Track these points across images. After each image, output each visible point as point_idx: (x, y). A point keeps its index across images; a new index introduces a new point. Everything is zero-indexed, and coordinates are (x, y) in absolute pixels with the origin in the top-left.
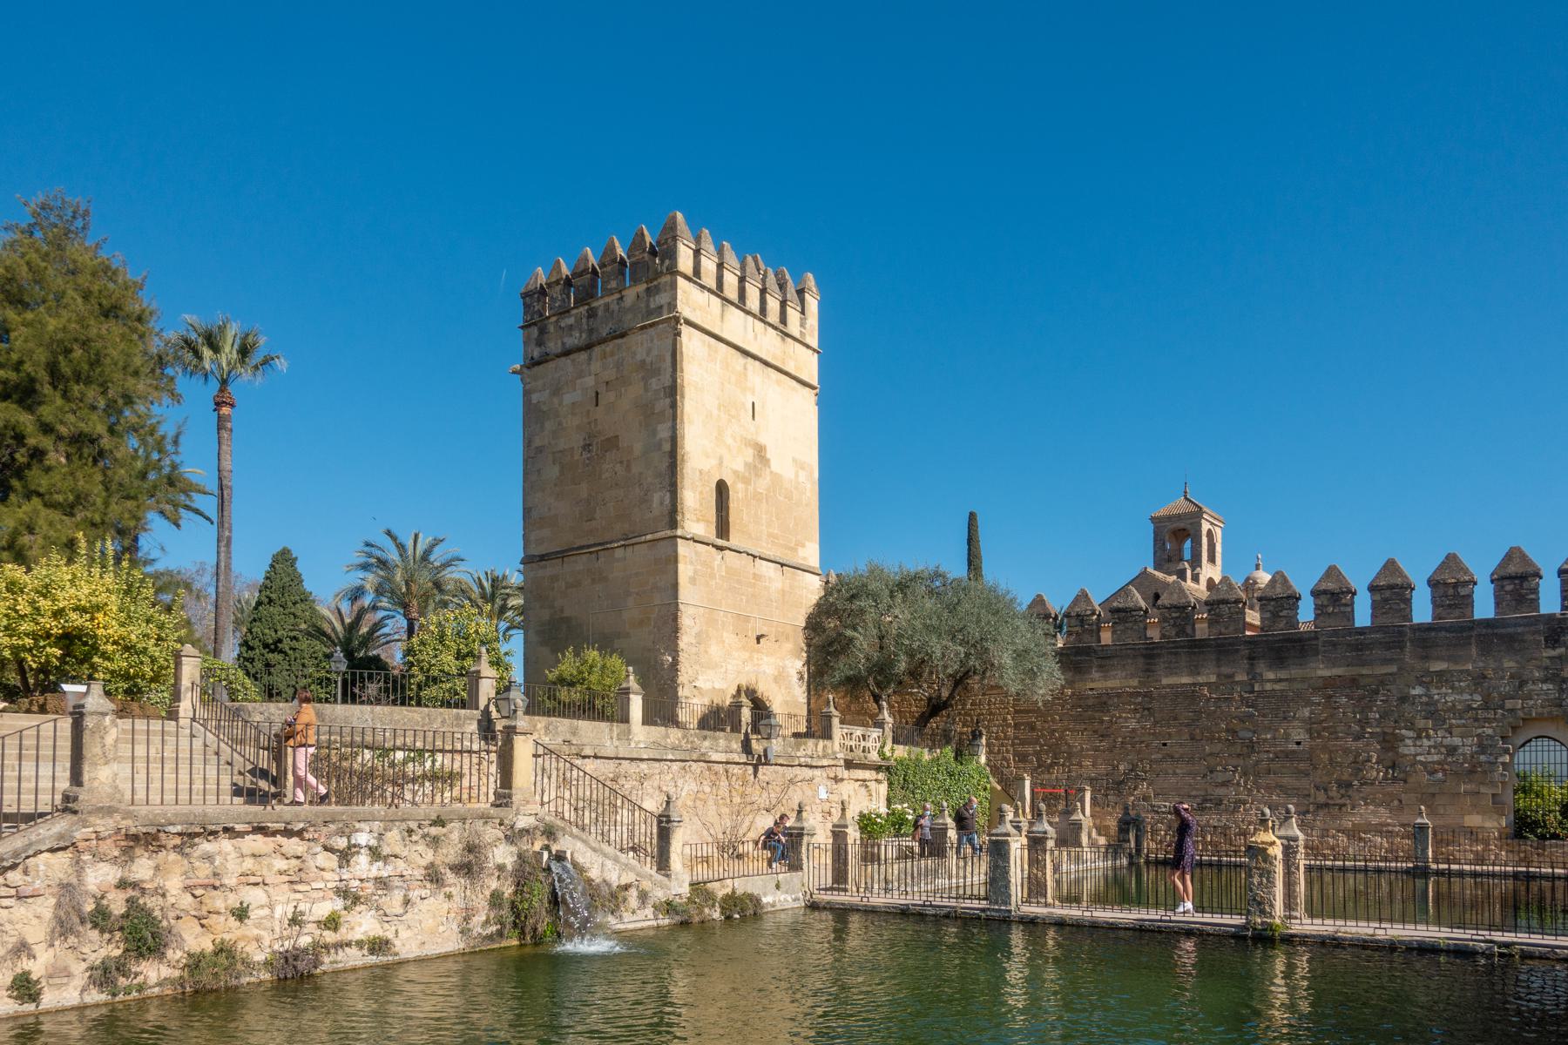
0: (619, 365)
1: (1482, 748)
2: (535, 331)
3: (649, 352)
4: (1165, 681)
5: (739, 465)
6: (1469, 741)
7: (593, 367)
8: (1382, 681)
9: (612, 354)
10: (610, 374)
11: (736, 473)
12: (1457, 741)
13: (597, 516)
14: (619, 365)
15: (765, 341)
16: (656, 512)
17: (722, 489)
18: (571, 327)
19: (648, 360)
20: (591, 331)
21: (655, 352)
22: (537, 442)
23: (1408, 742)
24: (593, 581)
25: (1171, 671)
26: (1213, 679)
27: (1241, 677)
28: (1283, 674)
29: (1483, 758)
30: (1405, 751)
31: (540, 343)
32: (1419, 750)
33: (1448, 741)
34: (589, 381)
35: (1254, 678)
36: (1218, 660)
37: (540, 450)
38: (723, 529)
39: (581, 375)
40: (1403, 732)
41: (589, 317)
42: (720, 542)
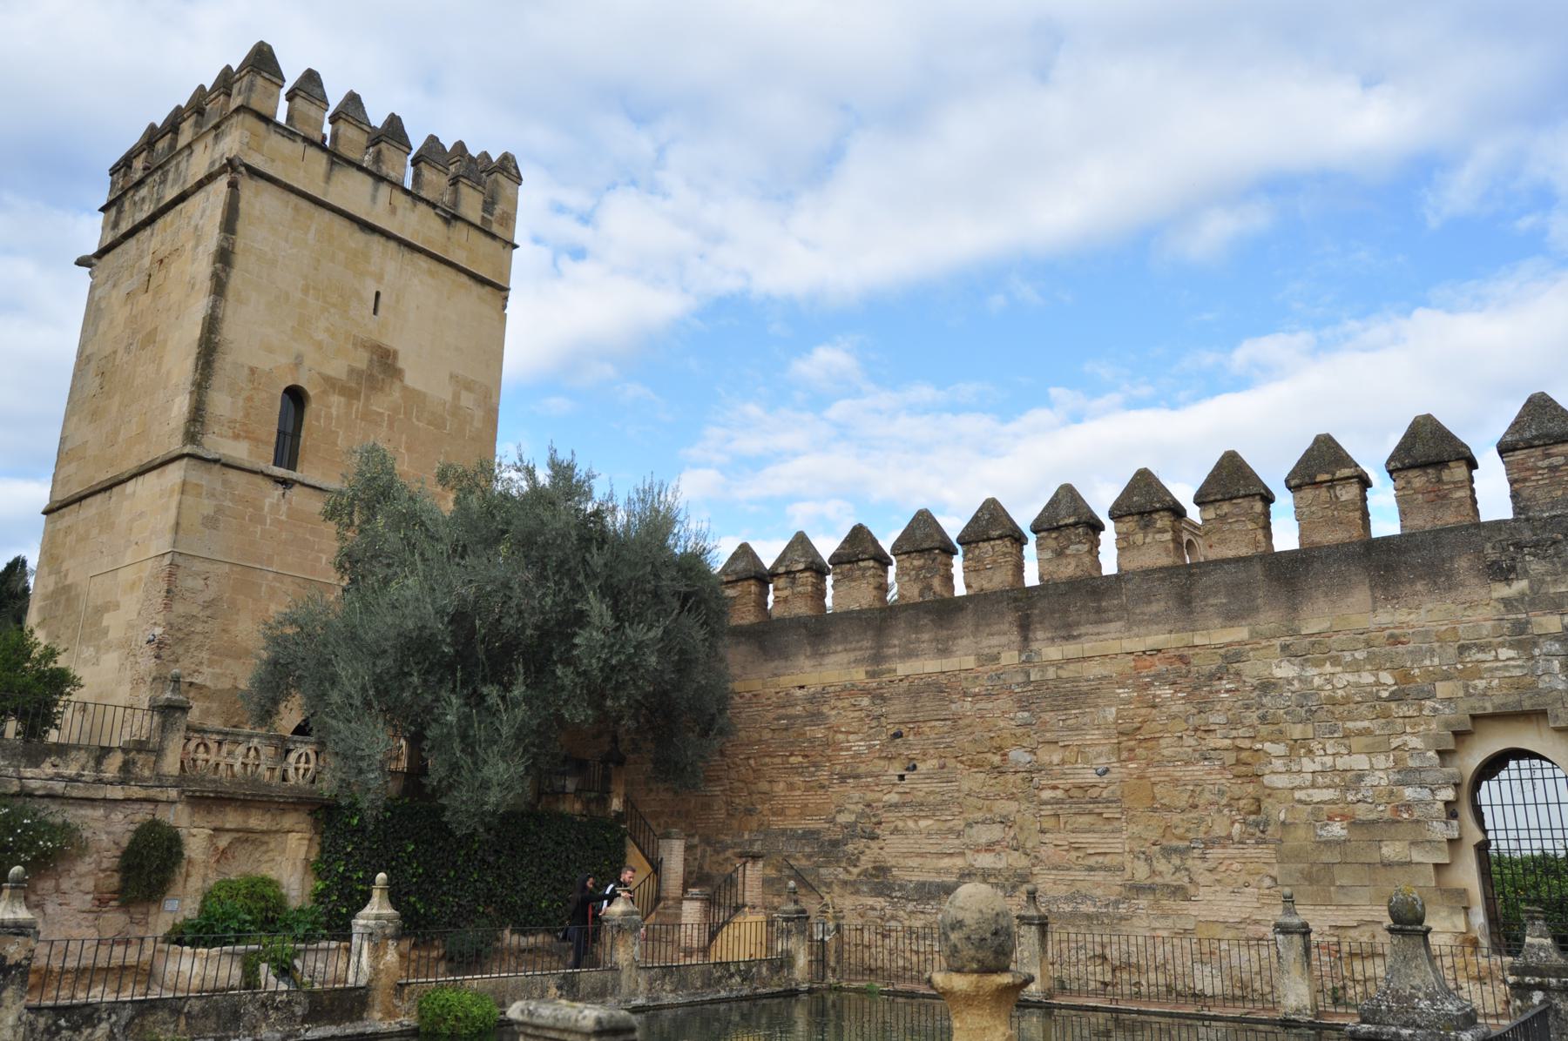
1: (1407, 776)
4: (902, 669)
5: (337, 368)
6: (1381, 761)
8: (1232, 656)
11: (330, 383)
12: (1360, 762)
23: (1278, 764)
25: (909, 654)
26: (970, 662)
27: (1010, 658)
28: (1072, 649)
29: (1409, 793)
30: (1280, 781)
32: (1298, 781)
33: (1341, 763)
35: (1028, 660)
36: (977, 626)
40: (1268, 746)
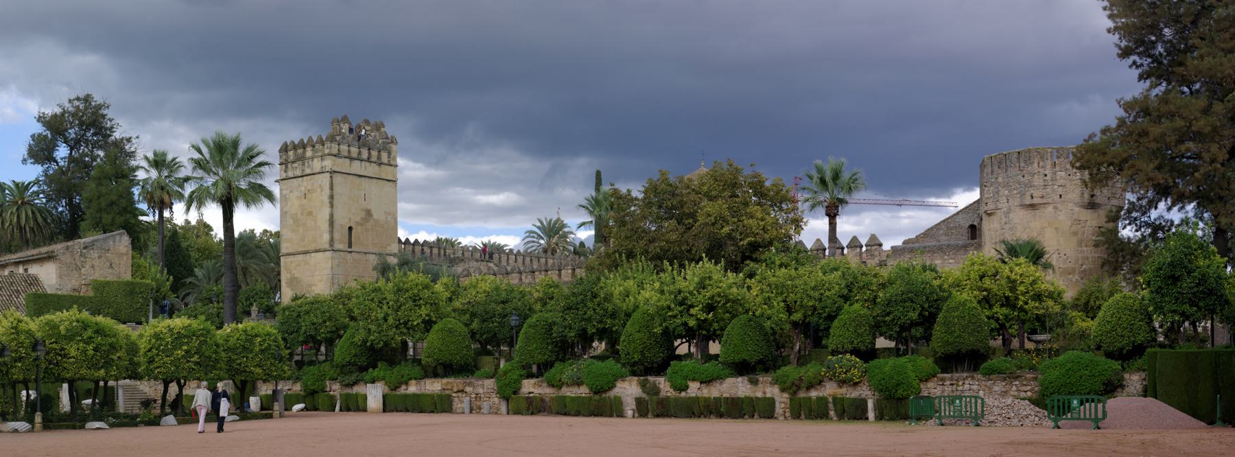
10: (309, 187)
11: (357, 223)
15: (371, 170)
38: (350, 246)
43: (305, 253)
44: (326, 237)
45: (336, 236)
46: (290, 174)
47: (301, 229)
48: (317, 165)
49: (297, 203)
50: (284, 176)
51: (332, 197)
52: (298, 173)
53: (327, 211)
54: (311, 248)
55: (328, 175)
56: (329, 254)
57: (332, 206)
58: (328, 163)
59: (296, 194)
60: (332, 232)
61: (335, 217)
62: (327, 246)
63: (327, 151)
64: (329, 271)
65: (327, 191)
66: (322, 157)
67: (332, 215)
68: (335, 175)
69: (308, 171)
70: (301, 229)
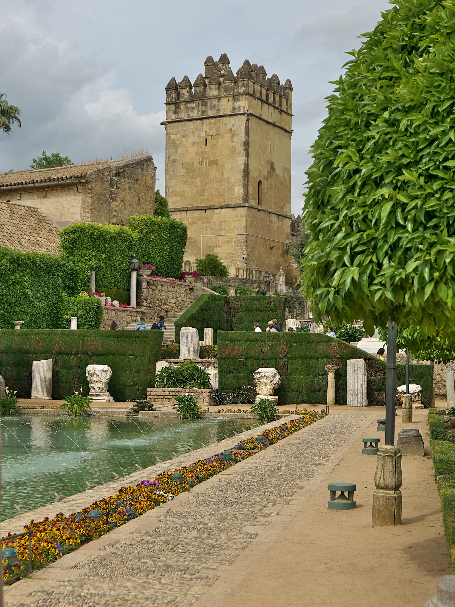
0: (218, 129)
2: (173, 107)
3: (233, 125)
7: (204, 127)
9: (215, 123)
13: (206, 193)
14: (218, 129)
16: (236, 195)
17: (260, 182)
18: (193, 108)
19: (233, 129)
20: (203, 112)
21: (237, 126)
22: (174, 157)
24: (203, 222)
31: (175, 112)
34: (203, 134)
37: (175, 161)
38: (259, 202)
39: (198, 130)
41: (202, 105)
42: (259, 207)
43: (205, 209)
44: (239, 190)
45: (251, 189)
46: (183, 115)
47: (199, 181)
48: (226, 106)
49: (193, 150)
50: (173, 117)
51: (247, 144)
52: (195, 114)
53: (241, 160)
54: (215, 202)
55: (244, 119)
56: (243, 211)
57: (247, 155)
58: (243, 104)
59: (191, 139)
60: (246, 186)
61: (251, 168)
62: (240, 201)
63: (242, 90)
64: (242, 231)
65: (243, 137)
66: (236, 97)
67: (247, 166)
68: (251, 118)
69: (211, 113)
70: (199, 181)
